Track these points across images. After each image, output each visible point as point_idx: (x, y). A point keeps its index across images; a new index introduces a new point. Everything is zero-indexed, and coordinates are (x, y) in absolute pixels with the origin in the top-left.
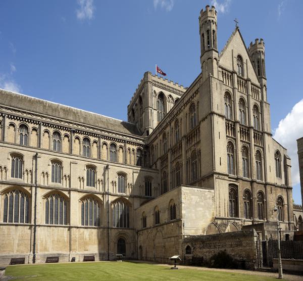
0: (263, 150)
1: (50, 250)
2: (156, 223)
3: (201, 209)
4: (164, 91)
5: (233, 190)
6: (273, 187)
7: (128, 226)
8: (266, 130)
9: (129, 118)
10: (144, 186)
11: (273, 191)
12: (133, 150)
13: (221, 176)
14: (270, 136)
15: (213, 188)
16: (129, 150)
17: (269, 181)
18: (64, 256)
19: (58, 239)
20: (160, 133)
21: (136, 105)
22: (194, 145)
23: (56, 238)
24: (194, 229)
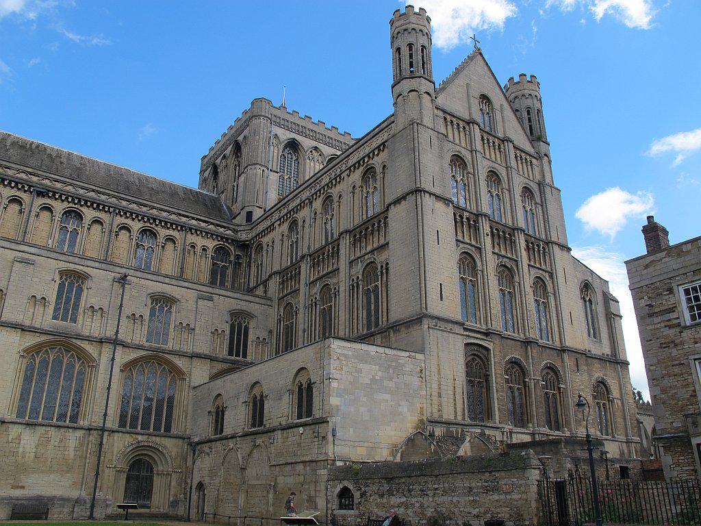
0: (551, 277)
2: (253, 425)
3: (388, 397)
4: (299, 138)
5: (477, 361)
6: (582, 360)
7: (168, 428)
8: (554, 239)
9: (204, 181)
10: (228, 332)
11: (583, 367)
13: (442, 325)
14: (565, 253)
15: (422, 351)
17: (569, 343)
20: (281, 220)
21: (224, 156)
22: (372, 252)
24: (366, 444)
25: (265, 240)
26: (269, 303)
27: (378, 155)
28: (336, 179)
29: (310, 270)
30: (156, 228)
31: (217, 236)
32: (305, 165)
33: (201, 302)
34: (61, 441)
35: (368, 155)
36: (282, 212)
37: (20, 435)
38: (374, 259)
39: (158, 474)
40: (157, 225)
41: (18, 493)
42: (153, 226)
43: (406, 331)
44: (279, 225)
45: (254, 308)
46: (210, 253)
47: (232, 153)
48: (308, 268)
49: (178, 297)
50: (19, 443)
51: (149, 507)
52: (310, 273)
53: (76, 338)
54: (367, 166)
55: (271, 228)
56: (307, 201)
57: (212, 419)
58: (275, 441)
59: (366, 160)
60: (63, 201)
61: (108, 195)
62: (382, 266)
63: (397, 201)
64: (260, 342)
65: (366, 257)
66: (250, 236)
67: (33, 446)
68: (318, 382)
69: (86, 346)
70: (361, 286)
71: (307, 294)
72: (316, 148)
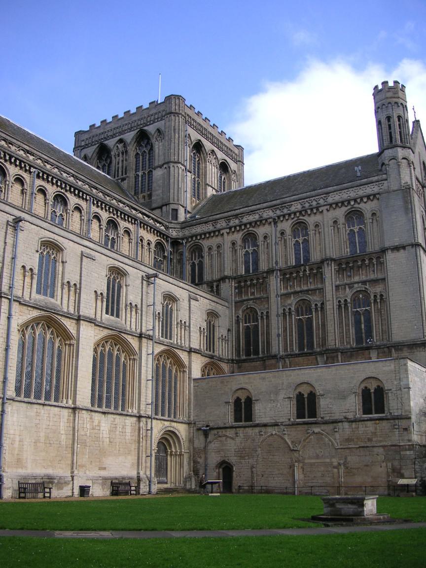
1: (29, 465)
12: (149, 244)
16: (141, 240)
18: (61, 483)
19: (47, 437)
20: (231, 229)
22: (364, 283)
23: (42, 434)
25: (205, 243)
26: (226, 304)
27: (365, 203)
28: (312, 210)
29: (280, 282)
30: (117, 219)
31: (158, 231)
32: (206, 167)
33: (193, 302)
34: (123, 428)
35: (355, 200)
36: (232, 222)
37: (99, 422)
38: (365, 288)
39: (171, 455)
40: (118, 216)
41: (104, 473)
42: (115, 217)
43: (409, 351)
44: (228, 233)
45: (220, 309)
46: (153, 246)
47: (135, 140)
48: (279, 282)
49: (178, 296)
50: (100, 430)
51: (166, 483)
52: (281, 285)
53: (125, 333)
54: (351, 208)
55: (217, 233)
56: (271, 220)
57: (231, 409)
58: (341, 430)
59: (352, 203)
60: (53, 184)
61: (83, 181)
62: (375, 296)
63: (396, 249)
64: (222, 338)
65: (356, 285)
66: (181, 235)
67: (107, 433)
68: (393, 389)
69: (129, 339)
70: (350, 308)
71: (279, 304)
72: (213, 151)
